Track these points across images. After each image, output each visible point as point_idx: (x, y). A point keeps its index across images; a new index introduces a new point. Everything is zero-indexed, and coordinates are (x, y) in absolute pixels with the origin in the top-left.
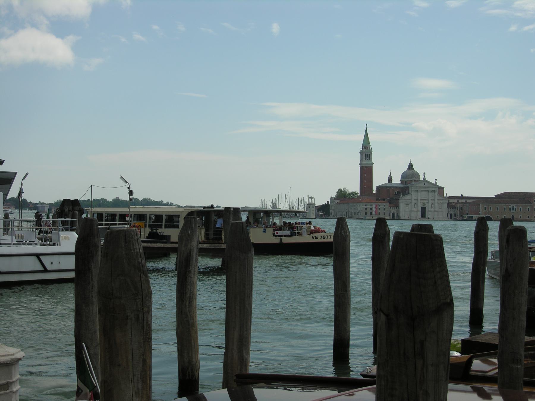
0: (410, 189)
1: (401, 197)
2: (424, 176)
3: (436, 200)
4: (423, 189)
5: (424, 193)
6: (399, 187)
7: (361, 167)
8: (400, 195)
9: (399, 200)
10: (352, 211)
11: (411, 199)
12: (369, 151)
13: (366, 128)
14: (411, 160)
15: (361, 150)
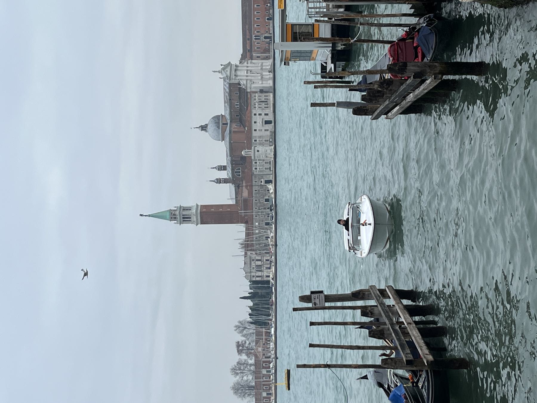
0: (233, 81)
1: (244, 87)
2: (216, 72)
3: (247, 65)
4: (233, 72)
5: (239, 73)
6: (230, 124)
7: (201, 220)
8: (241, 88)
9: (247, 92)
10: (264, 160)
11: (247, 80)
12: (179, 209)
13: (146, 216)
14: (195, 128)
15: (177, 224)
